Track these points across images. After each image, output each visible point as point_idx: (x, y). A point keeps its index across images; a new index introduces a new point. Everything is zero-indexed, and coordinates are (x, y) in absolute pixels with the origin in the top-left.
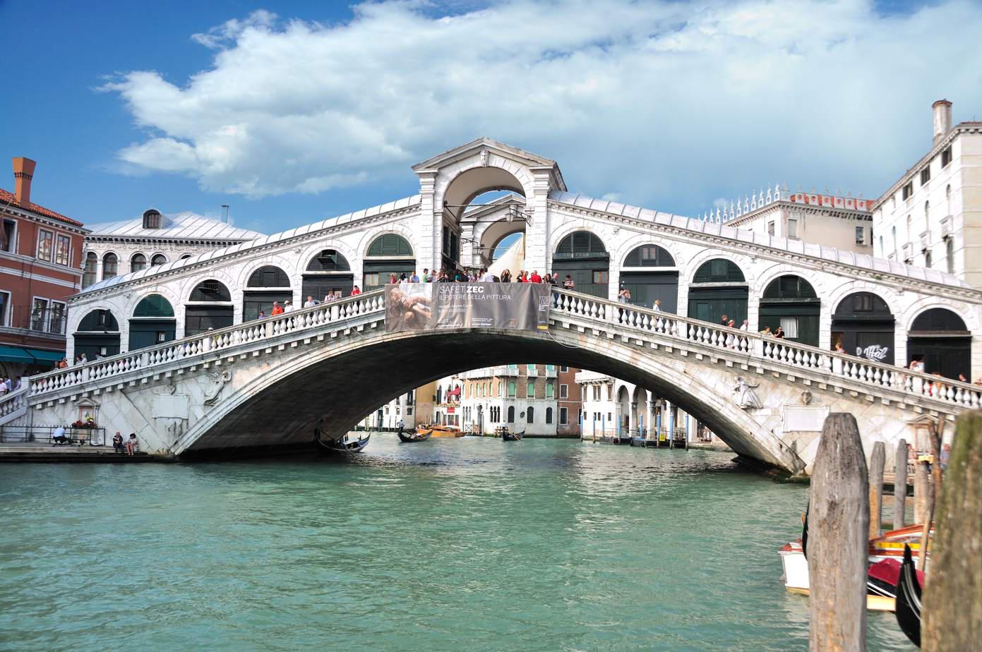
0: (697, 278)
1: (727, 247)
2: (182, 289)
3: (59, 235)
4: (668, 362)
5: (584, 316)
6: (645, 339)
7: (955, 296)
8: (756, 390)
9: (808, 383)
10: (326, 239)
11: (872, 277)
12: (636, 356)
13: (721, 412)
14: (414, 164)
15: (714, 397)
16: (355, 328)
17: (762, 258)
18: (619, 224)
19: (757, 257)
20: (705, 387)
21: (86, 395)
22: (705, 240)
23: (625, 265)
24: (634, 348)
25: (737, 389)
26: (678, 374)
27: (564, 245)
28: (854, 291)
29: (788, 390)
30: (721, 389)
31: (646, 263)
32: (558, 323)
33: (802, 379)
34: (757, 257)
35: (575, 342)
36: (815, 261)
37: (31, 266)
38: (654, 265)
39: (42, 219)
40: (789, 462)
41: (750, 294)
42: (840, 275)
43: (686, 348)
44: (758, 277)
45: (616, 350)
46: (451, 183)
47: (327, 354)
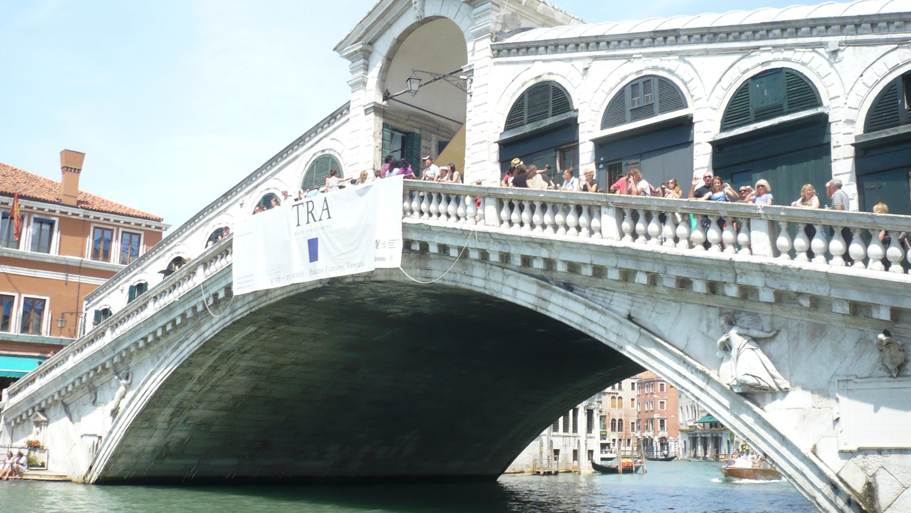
3: (123, 232)
6: (545, 253)
9: (884, 315)
10: (265, 180)
12: (545, 293)
14: (334, 46)
16: (215, 295)
22: (736, 39)
23: (605, 124)
24: (542, 278)
26: (611, 323)
31: (639, 113)
32: (424, 247)
33: (868, 307)
35: (458, 277)
37: (80, 268)
38: (652, 114)
39: (92, 214)
41: (834, 129)
45: (514, 286)
46: (389, 59)
47: (202, 337)
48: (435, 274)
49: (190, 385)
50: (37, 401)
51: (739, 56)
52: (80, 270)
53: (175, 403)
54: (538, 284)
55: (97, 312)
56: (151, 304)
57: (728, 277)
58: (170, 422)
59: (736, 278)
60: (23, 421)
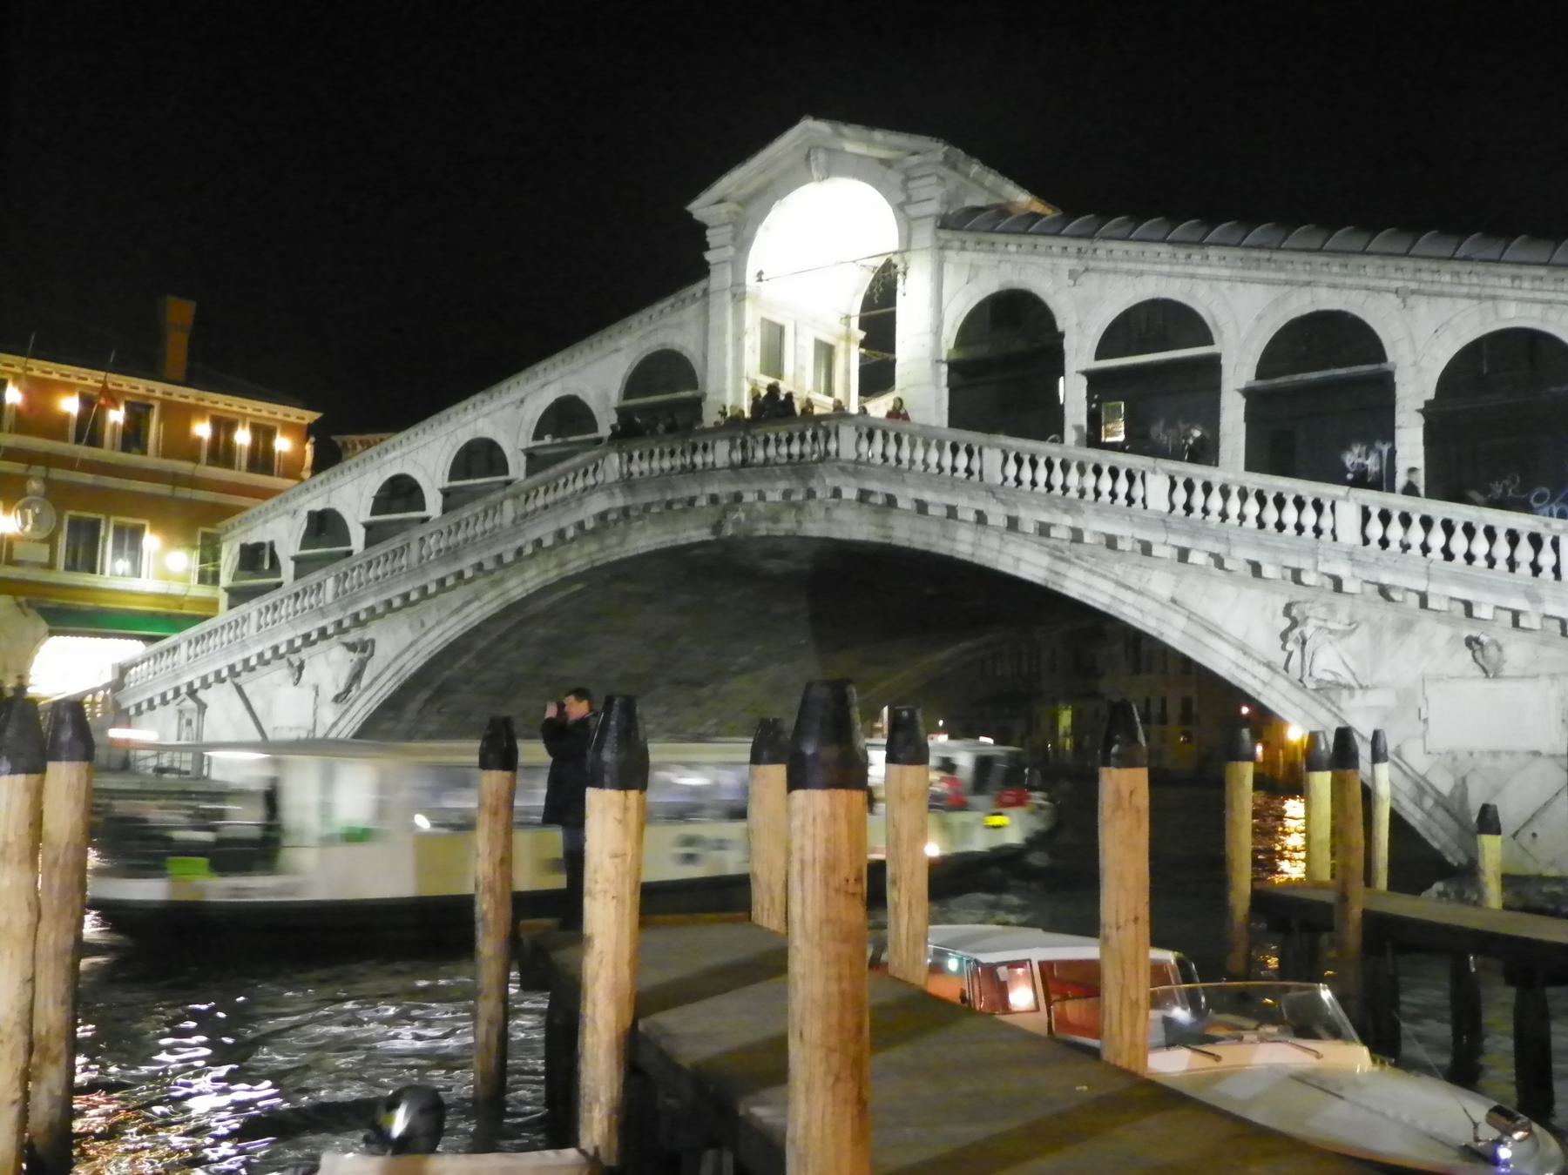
0: (1263, 370)
1: (1339, 280)
2: (361, 495)
12: (1061, 567)
17: (1430, 295)
21: (184, 690)
23: (1098, 357)
26: (1149, 605)
27: (971, 328)
35: (933, 539)
49: (464, 661)
50: (187, 679)
51: (1287, 288)
52: (193, 482)
53: (436, 684)
54: (1051, 555)
55: (244, 548)
56: (415, 547)
57: (1305, 563)
58: (420, 711)
59: (1317, 563)
60: (151, 706)
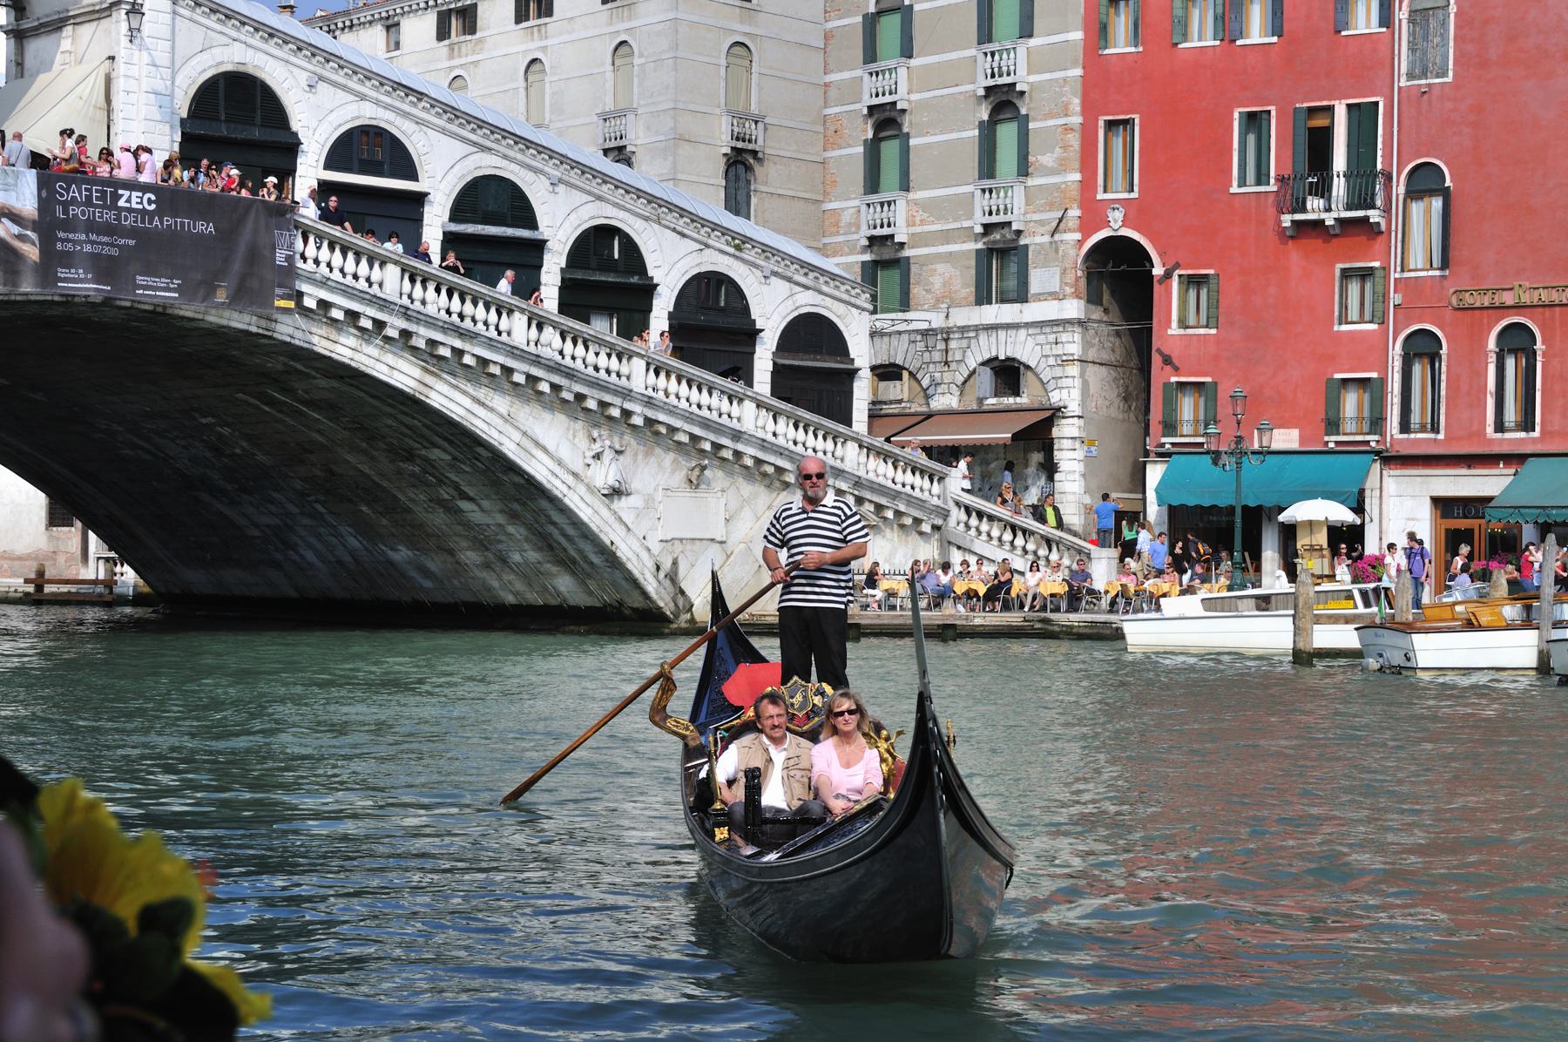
1: (511, 153)
4: (481, 393)
5: (358, 286)
6: (458, 344)
7: (837, 293)
8: (621, 458)
11: (728, 243)
12: (429, 380)
13: (566, 501)
15: (557, 470)
18: (319, 70)
19: (560, 181)
20: (545, 450)
22: (473, 130)
23: (329, 165)
25: (597, 456)
28: (703, 269)
29: (669, 458)
30: (565, 453)
34: (560, 181)
35: (315, 340)
36: (649, 202)
40: (668, 599)
41: (547, 257)
42: (684, 235)
43: (524, 367)
44: (560, 220)
48: (280, 327)
